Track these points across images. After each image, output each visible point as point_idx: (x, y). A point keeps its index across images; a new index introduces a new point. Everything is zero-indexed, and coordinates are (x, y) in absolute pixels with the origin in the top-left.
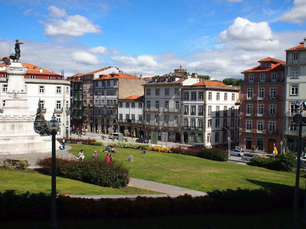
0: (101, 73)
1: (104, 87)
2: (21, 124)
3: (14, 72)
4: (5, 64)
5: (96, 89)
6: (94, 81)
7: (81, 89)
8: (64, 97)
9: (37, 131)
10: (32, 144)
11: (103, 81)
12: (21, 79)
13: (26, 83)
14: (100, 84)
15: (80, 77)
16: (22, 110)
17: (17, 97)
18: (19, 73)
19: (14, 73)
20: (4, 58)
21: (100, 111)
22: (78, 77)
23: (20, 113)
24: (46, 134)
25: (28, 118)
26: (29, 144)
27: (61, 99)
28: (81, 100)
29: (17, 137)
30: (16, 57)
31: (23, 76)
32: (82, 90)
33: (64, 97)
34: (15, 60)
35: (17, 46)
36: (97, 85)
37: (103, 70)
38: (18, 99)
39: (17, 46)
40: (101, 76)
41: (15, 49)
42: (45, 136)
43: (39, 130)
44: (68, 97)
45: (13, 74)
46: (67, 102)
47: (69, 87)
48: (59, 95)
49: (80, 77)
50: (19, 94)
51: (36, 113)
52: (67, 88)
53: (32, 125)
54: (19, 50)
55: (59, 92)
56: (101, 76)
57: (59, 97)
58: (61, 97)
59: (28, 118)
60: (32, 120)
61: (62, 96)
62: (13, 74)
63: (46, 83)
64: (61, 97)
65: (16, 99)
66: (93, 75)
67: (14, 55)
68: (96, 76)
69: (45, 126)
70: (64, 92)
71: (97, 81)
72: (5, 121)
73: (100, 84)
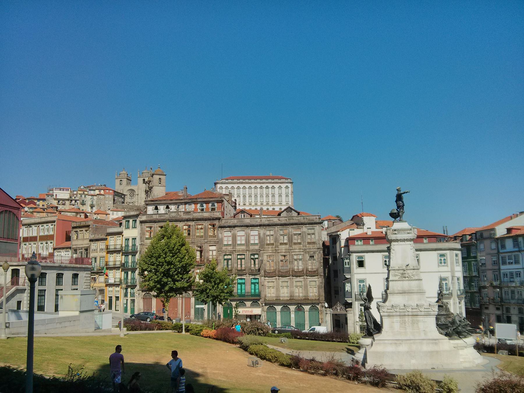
0: (510, 224)
1: (517, 249)
2: (415, 318)
3: (399, 236)
4: (356, 226)
5: (502, 253)
6: (498, 239)
7: (472, 255)
8: (452, 271)
9: (440, 330)
10: (437, 352)
11: (515, 238)
12: (409, 247)
13: (417, 250)
14: (509, 245)
15: (470, 235)
16: (415, 297)
17: (406, 275)
18: (406, 238)
19: (399, 239)
20: (354, 217)
21: (514, 294)
22: (466, 235)
23: (413, 301)
24: (456, 337)
25: (426, 310)
26: (432, 354)
27: (448, 275)
28: (475, 274)
29: (412, 342)
30: (398, 213)
31: (412, 242)
32: (475, 257)
33: (452, 271)
34: (397, 219)
35: (399, 198)
36: (503, 247)
37: (511, 218)
38: (407, 279)
39: (399, 198)
40: (509, 230)
41: (396, 201)
42: (455, 339)
43: (442, 329)
44: (459, 271)
45: (397, 240)
46: (458, 279)
47: (459, 253)
48: (445, 269)
49: (470, 235)
50: (409, 271)
51: (437, 299)
52: (456, 255)
53: (432, 322)
54: (403, 202)
55: (443, 264)
56: (509, 230)
57: (445, 272)
58: (448, 272)
59: (426, 310)
60: (432, 313)
61: (448, 269)
62: (397, 240)
63: (421, 250)
64: (448, 272)
65: (404, 279)
66: (493, 229)
67: (396, 211)
68: (501, 231)
69: (453, 322)
70: (452, 263)
71: (502, 239)
72: (415, 313)
73: (509, 245)
